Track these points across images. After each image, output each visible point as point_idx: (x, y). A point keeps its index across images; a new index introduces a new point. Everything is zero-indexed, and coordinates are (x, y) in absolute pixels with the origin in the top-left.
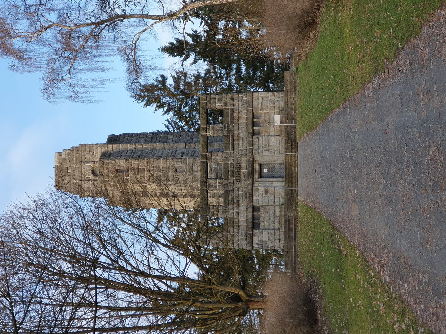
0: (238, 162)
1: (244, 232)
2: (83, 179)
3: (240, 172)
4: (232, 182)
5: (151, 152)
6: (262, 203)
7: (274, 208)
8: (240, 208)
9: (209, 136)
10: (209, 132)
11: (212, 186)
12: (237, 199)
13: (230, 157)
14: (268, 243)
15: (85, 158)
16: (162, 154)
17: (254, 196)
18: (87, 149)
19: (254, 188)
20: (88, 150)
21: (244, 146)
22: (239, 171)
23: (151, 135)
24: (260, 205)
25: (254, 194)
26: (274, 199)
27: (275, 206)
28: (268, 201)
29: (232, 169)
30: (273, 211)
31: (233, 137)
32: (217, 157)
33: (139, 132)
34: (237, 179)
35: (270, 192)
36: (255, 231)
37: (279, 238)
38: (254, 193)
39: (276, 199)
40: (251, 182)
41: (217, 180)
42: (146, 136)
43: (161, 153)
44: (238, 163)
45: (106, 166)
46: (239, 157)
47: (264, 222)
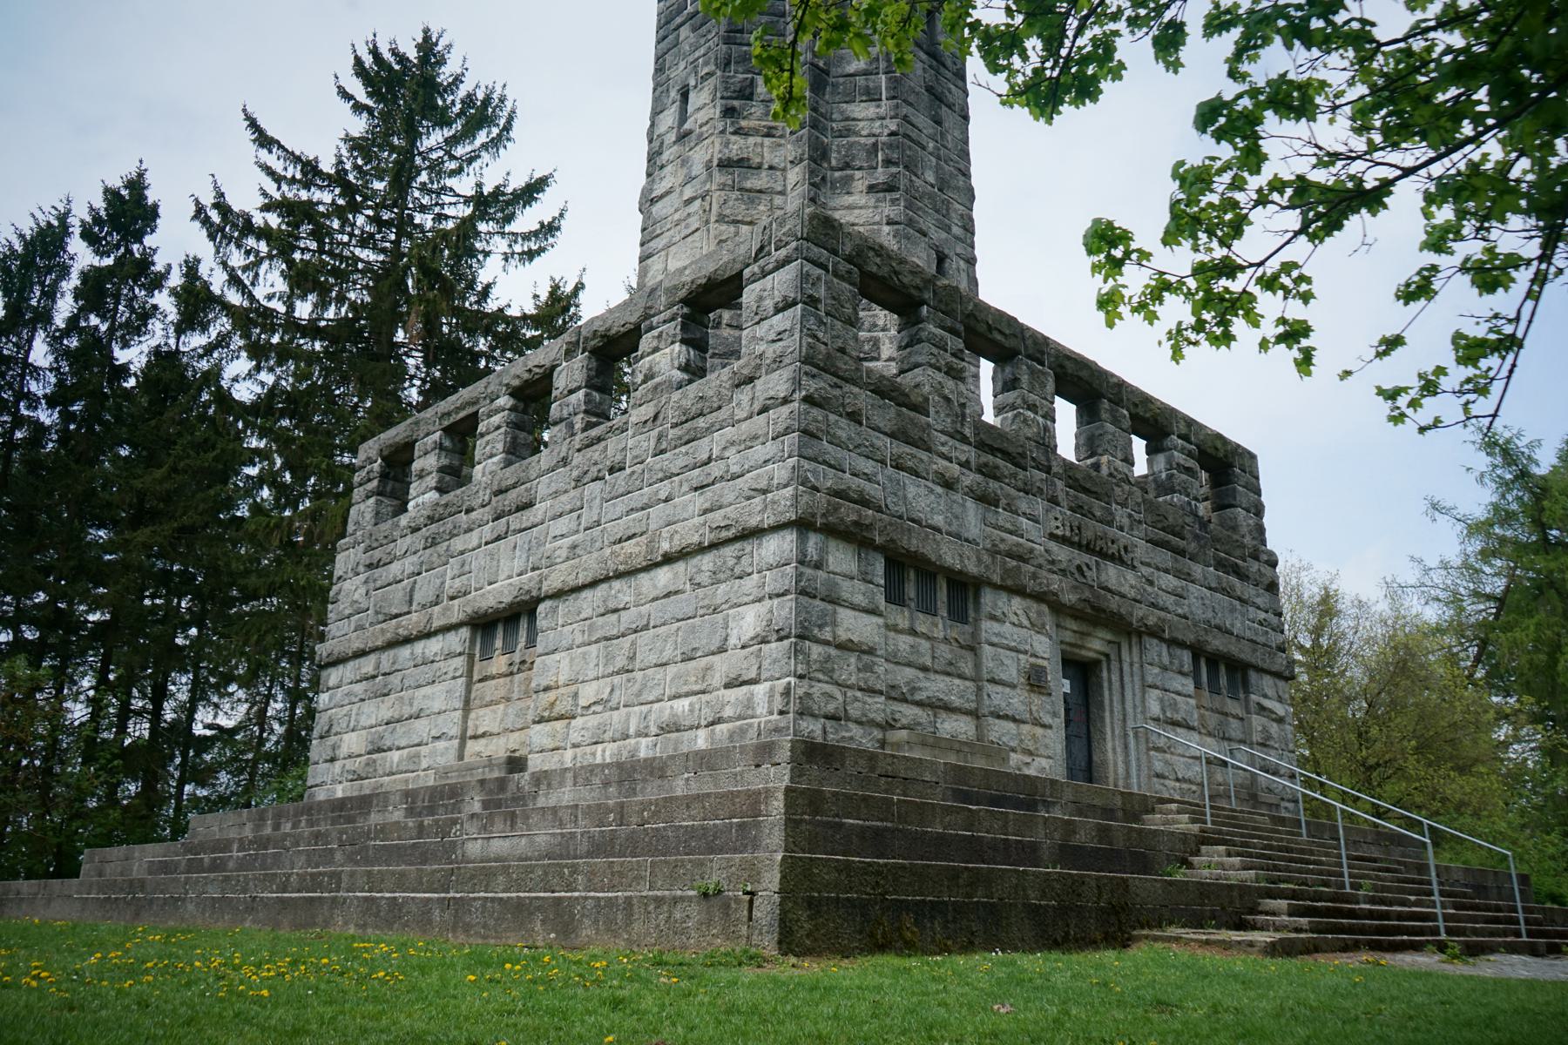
1: (872, 490)
6: (995, 640)
7: (967, 705)
8: (970, 504)
14: (827, 634)
24: (987, 626)
26: (1014, 720)
27: (975, 714)
28: (1003, 677)
30: (956, 701)
35: (1037, 700)
36: (879, 567)
37: (848, 719)
39: (1012, 725)
40: (1069, 598)
47: (913, 632)
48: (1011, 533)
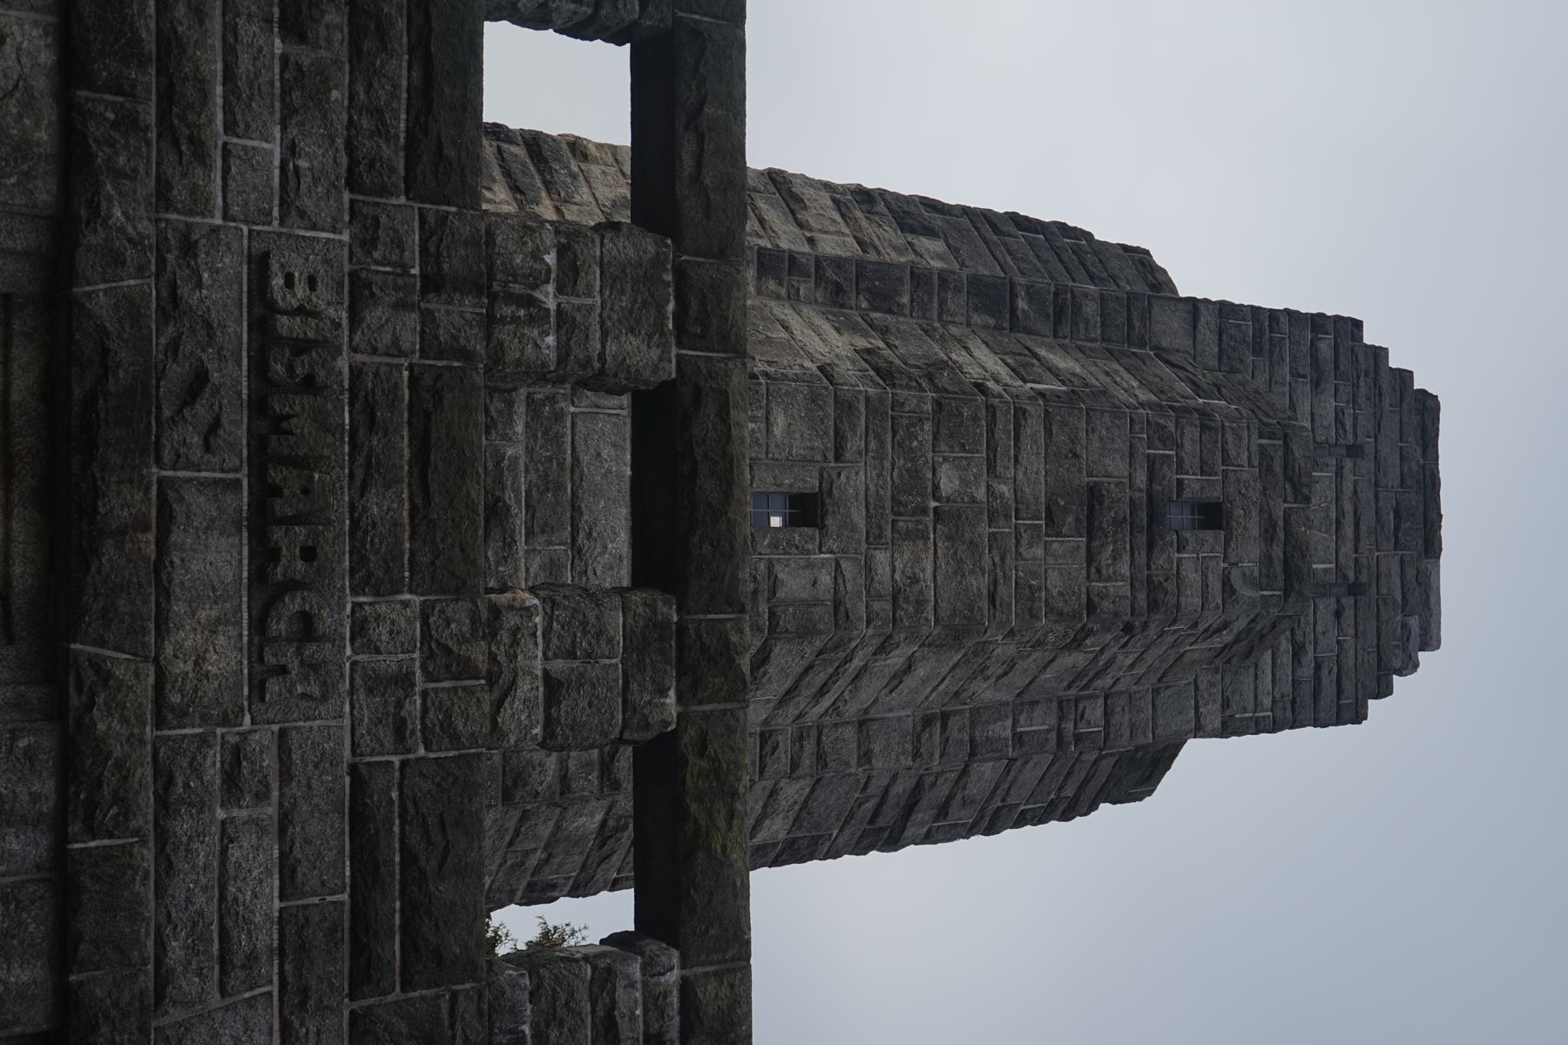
0: (293, 604)
2: (1348, 464)
3: (261, 457)
4: (374, 316)
5: (974, 686)
9: (652, 946)
10: (654, 1001)
11: (614, 277)
12: (305, 56)
13: (404, 680)
15: (1338, 614)
16: (909, 667)
17: (46, 57)
18: (1328, 682)
19: (45, 192)
20: (1324, 673)
21: (205, 851)
22: (275, 475)
23: (908, 833)
25: (41, 83)
29: (375, 505)
31: (364, 974)
32: (559, 666)
33: (978, 843)
34: (302, 347)
38: (49, 112)
41: (563, 355)
42: (943, 811)
43: (909, 682)
44: (293, 585)
45: (1277, 551)
46: (274, 686)
48: (229, 76)
